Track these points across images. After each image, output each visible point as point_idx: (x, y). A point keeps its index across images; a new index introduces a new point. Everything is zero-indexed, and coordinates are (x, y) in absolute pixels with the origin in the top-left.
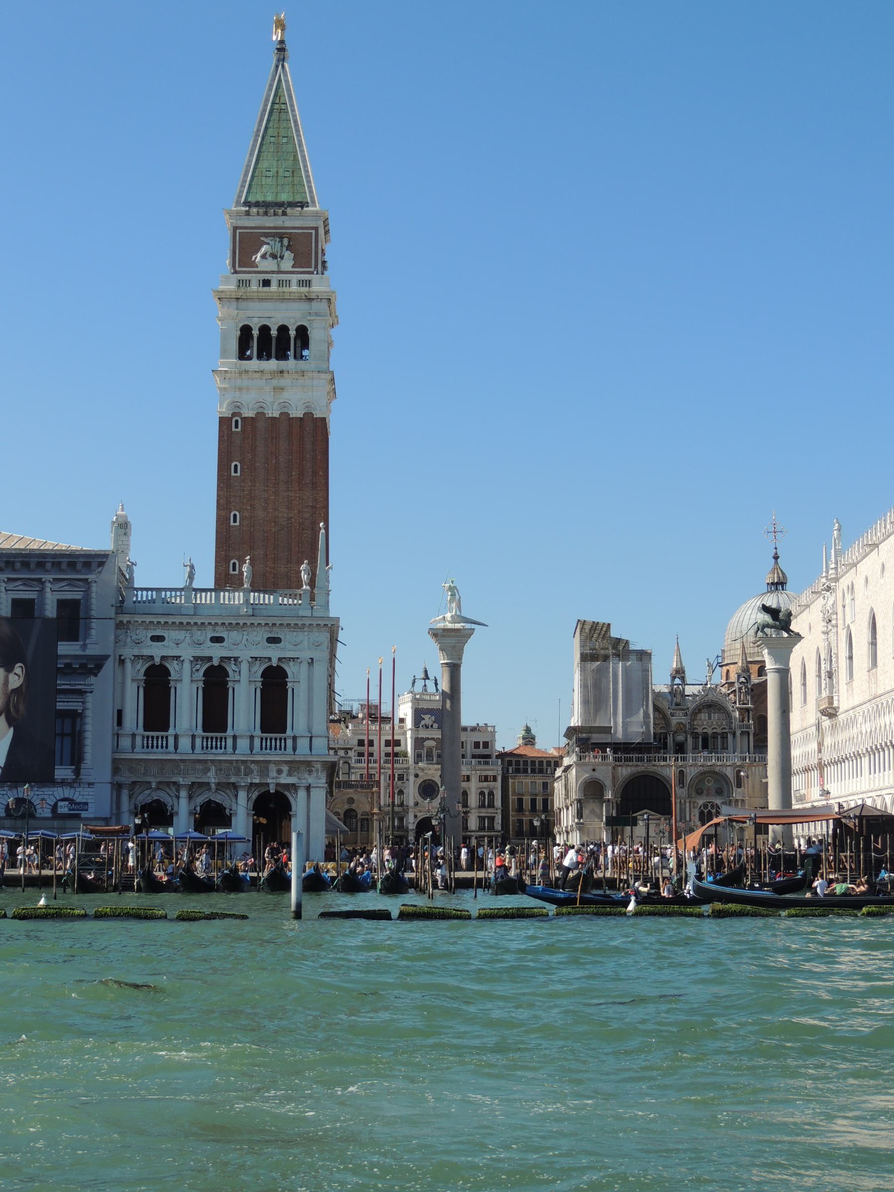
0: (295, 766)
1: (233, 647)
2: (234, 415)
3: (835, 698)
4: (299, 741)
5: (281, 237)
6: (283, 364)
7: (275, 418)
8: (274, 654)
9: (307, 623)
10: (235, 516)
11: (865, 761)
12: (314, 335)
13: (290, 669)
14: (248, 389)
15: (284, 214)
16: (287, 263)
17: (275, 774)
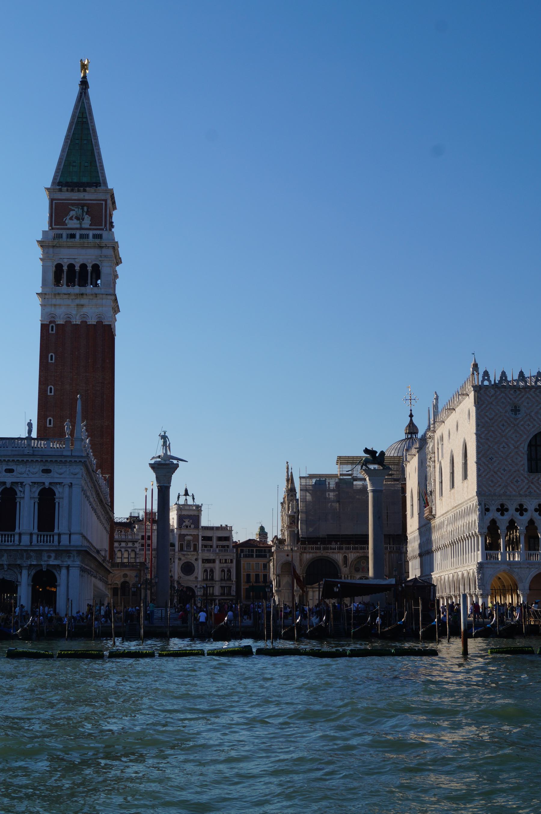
0: (61, 553)
1: (19, 476)
2: (51, 322)
3: (434, 509)
4: (63, 537)
5: (83, 206)
6: (83, 290)
7: (78, 324)
8: (47, 480)
9: (68, 460)
10: (51, 388)
11: (449, 549)
12: (105, 270)
13: (58, 490)
14: (60, 305)
15: (85, 191)
16: (87, 222)
17: (46, 559)
